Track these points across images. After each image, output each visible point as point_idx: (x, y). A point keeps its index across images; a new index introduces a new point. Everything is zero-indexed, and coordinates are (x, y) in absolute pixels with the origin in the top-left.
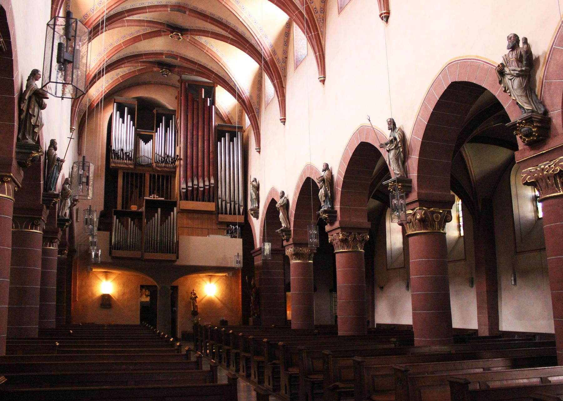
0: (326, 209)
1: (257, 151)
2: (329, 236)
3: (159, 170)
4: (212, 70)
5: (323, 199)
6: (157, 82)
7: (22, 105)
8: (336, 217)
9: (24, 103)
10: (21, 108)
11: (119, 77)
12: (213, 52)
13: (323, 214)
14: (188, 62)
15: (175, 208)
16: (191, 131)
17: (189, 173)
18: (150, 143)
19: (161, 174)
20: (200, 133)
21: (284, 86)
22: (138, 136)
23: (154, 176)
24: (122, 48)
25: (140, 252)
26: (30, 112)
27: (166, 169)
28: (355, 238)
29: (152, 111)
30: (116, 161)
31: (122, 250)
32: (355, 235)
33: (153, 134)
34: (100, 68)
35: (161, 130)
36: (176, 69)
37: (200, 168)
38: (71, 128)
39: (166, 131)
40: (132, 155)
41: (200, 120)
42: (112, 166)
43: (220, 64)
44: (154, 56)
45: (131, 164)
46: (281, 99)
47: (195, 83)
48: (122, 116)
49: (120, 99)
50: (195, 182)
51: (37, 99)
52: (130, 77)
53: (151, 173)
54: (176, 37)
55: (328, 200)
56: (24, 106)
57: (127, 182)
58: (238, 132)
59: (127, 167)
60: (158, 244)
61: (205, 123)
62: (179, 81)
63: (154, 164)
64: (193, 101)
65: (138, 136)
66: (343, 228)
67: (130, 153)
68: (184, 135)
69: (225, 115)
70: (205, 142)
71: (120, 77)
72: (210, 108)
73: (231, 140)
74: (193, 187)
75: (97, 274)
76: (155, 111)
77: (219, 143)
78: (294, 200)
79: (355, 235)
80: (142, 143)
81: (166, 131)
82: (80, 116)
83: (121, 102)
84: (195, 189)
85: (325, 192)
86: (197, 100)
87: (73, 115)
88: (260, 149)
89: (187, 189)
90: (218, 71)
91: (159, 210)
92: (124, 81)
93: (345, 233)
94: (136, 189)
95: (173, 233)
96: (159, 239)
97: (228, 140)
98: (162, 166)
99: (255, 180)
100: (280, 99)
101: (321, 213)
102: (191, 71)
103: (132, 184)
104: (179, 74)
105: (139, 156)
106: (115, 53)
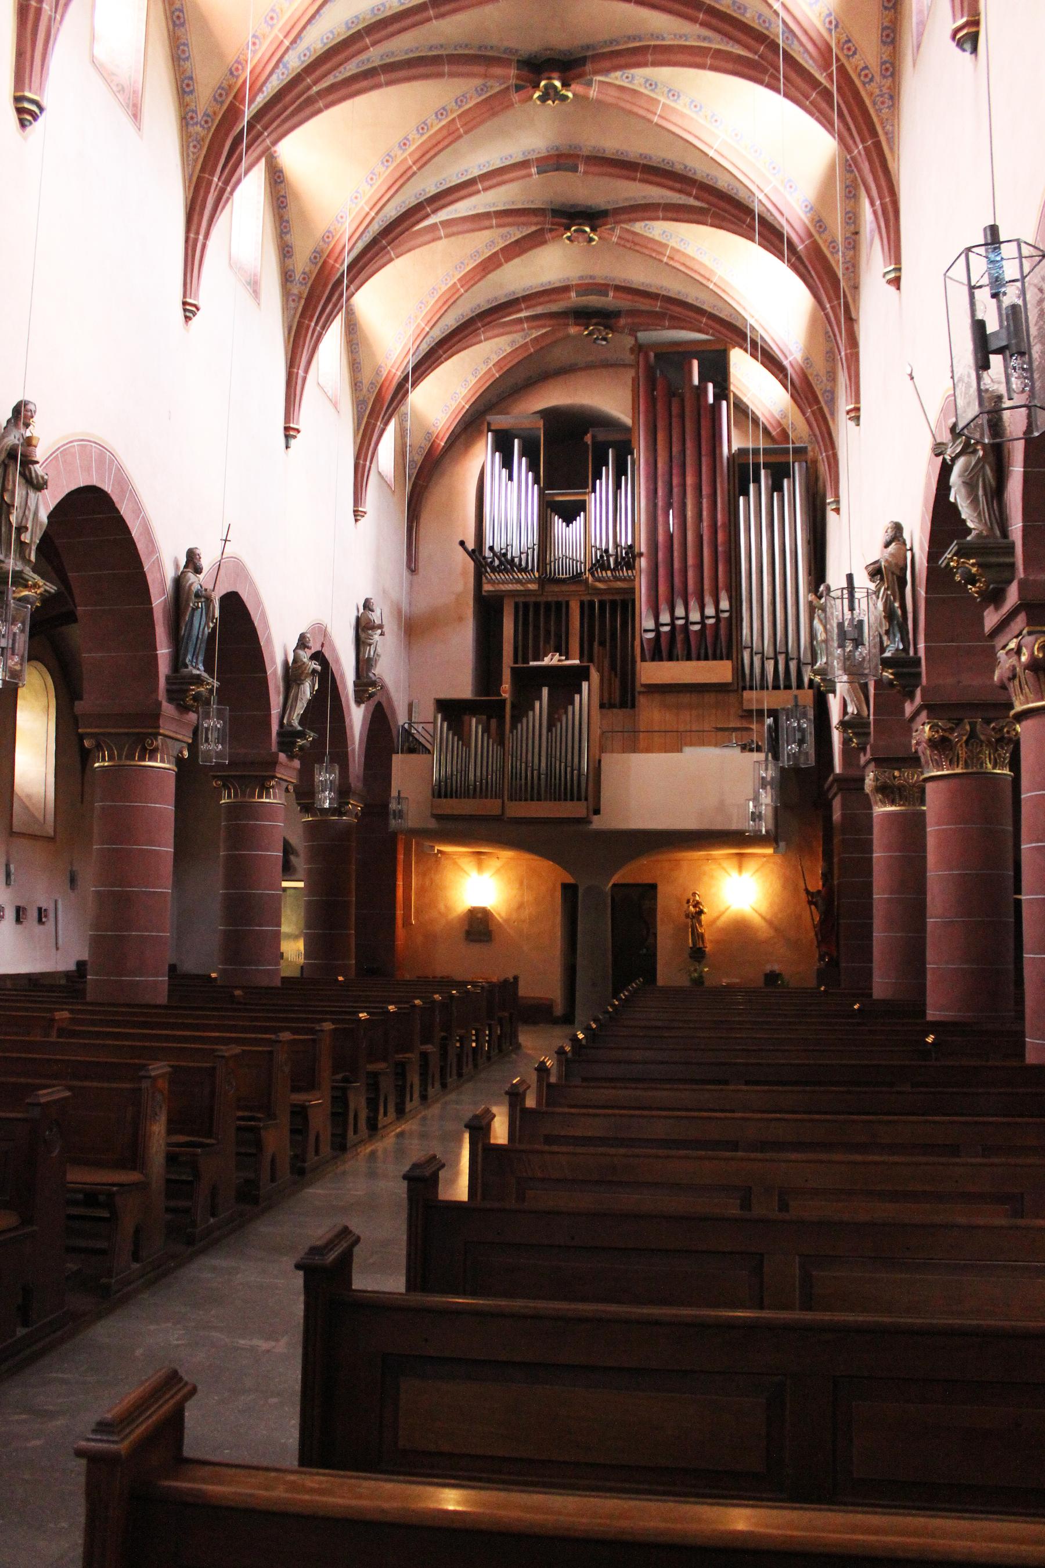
3: (600, 589)
4: (698, 305)
6: (592, 361)
8: (919, 675)
11: (491, 365)
12: (689, 257)
15: (584, 683)
16: (667, 477)
17: (662, 589)
18: (580, 521)
19: (611, 597)
20: (690, 480)
21: (854, 316)
22: (547, 507)
23: (591, 603)
25: (500, 801)
29: (582, 438)
31: (456, 797)
32: (973, 725)
33: (587, 498)
36: (622, 321)
37: (691, 574)
38: (355, 511)
39: (618, 486)
42: (486, 591)
43: (711, 286)
44: (547, 299)
45: (530, 581)
46: (846, 355)
48: (507, 463)
49: (500, 421)
50: (680, 611)
52: (516, 360)
54: (581, 239)
55: (896, 629)
58: (793, 463)
59: (522, 588)
61: (703, 452)
62: (632, 350)
65: (547, 507)
67: (530, 551)
68: (647, 489)
69: (771, 420)
70: (705, 501)
71: (494, 365)
72: (715, 409)
73: (776, 487)
74: (672, 624)
75: (459, 858)
76: (588, 439)
77: (741, 498)
79: (973, 725)
80: (558, 524)
81: (618, 486)
84: (678, 629)
87: (359, 479)
89: (657, 630)
90: (715, 306)
91: (545, 691)
92: (505, 373)
95: (580, 747)
96: (543, 765)
97: (766, 488)
102: (657, 319)
104: (633, 332)
105: (552, 559)
106: (442, 311)
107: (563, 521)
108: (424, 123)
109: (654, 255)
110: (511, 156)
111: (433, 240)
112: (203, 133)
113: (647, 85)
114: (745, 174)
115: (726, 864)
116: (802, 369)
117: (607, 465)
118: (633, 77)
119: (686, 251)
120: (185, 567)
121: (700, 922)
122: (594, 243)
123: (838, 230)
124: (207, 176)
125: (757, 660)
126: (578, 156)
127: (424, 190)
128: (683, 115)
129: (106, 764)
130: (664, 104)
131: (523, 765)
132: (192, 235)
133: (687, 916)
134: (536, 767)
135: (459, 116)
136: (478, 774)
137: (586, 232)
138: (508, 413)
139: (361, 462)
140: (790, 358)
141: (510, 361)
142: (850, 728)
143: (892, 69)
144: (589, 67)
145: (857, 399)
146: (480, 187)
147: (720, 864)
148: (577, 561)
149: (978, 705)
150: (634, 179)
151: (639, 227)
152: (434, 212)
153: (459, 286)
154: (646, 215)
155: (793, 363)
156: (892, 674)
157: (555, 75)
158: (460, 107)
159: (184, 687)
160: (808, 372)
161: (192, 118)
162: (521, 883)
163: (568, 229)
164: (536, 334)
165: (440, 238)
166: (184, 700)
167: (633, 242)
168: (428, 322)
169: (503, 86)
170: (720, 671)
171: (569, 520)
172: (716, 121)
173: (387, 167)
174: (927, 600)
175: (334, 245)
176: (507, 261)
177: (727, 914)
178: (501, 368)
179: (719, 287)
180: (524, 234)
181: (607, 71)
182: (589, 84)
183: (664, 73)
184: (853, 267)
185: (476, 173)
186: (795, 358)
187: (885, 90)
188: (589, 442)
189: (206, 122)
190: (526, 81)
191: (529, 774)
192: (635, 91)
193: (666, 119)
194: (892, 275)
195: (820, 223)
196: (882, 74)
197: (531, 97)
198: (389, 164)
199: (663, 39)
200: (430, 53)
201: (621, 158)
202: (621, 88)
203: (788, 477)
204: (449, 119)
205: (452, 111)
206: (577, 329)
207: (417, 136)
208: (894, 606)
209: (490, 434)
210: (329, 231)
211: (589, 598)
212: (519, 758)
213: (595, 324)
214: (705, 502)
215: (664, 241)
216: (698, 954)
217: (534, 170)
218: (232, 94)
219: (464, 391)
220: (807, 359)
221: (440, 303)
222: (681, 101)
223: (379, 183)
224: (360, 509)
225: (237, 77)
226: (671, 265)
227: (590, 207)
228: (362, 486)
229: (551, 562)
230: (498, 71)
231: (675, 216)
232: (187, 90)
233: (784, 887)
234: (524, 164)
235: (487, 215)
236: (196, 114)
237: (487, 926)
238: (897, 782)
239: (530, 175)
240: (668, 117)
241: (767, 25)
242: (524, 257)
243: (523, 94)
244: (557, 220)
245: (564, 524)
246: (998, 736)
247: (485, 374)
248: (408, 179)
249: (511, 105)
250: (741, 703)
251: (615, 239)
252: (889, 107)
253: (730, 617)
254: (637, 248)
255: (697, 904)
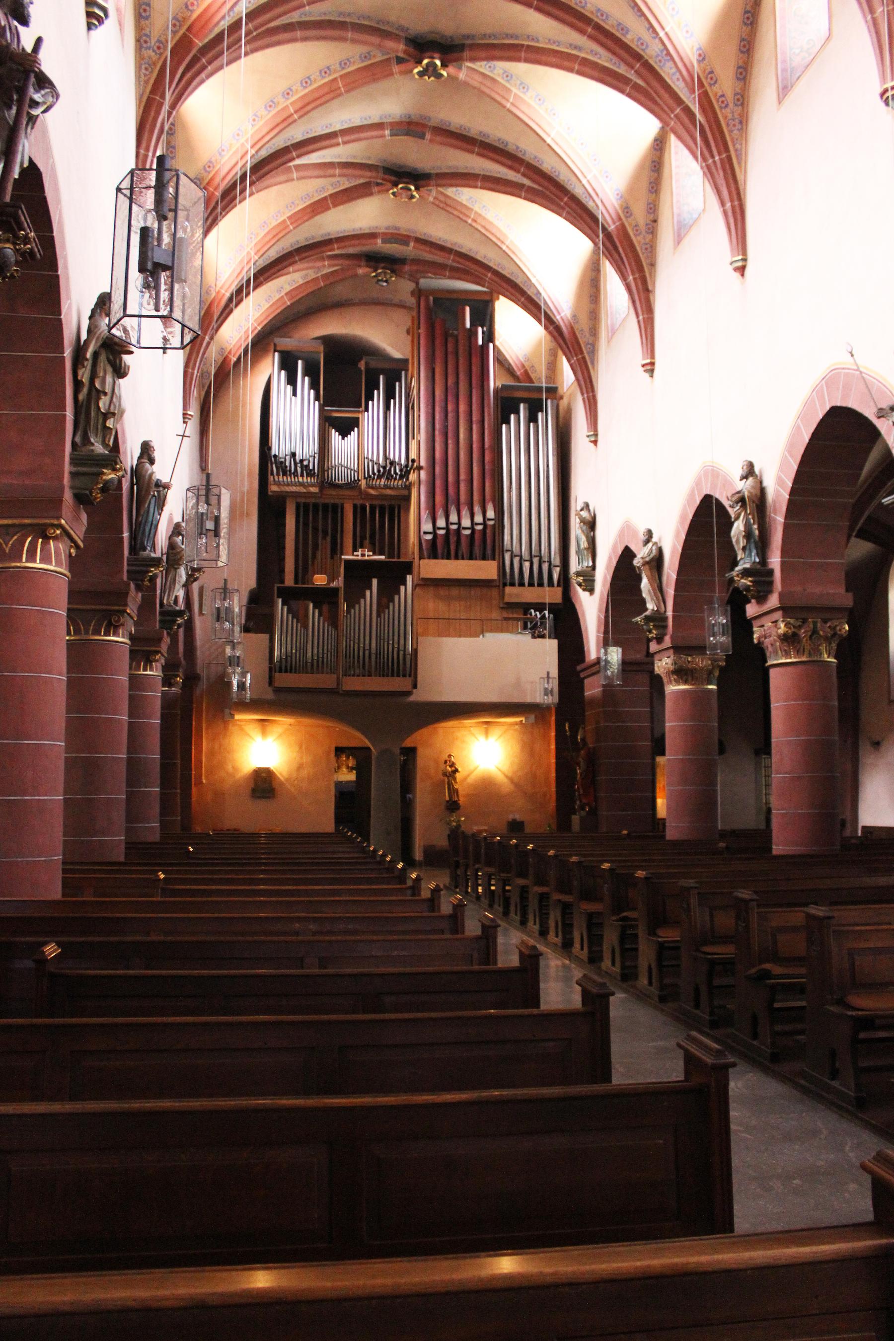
0: (748, 566)
1: (591, 442)
2: (755, 629)
3: (372, 495)
5: (742, 542)
7: (80, 372)
8: (771, 583)
9: (84, 366)
10: (79, 378)
11: (283, 294)
13: (742, 578)
14: (432, 250)
16: (443, 404)
17: (439, 498)
18: (354, 434)
20: (462, 408)
21: (650, 288)
23: (363, 508)
24: (287, 230)
26: (98, 385)
27: (389, 492)
28: (815, 632)
30: (281, 479)
32: (815, 623)
33: (360, 416)
34: (243, 278)
35: (377, 405)
36: (407, 268)
37: (463, 487)
38: (184, 414)
39: (387, 407)
40: (314, 464)
41: (462, 376)
42: (272, 491)
43: (504, 248)
45: (312, 485)
46: (644, 318)
47: (448, 296)
48: (292, 381)
49: (287, 343)
50: (453, 518)
51: (111, 357)
53: (355, 502)
55: (753, 546)
56: (84, 375)
57: (306, 524)
59: (304, 490)
60: (373, 657)
61: (474, 385)
62: (413, 293)
63: (363, 483)
64: (446, 336)
66: (786, 609)
67: (311, 459)
68: (427, 413)
72: (484, 349)
73: (532, 418)
74: (447, 528)
76: (362, 365)
77: (504, 426)
78: (674, 547)
79: (815, 623)
80: (335, 436)
81: (387, 407)
82: (203, 387)
83: (289, 348)
84: (452, 532)
85: (745, 528)
86: (455, 332)
87: (188, 386)
88: (596, 435)
89: (434, 533)
91: (375, 582)
93: (792, 621)
94: (324, 538)
97: (524, 418)
98: (379, 485)
99: (587, 506)
100: (641, 317)
101: (738, 575)
102: (439, 269)
103: (315, 529)
107: (340, 434)
108: (309, 78)
109: (461, 216)
110: (370, 118)
111: (287, 181)
112: (155, 57)
113: (505, 76)
114: (573, 162)
115: (474, 730)
116: (570, 324)
117: (378, 389)
118: (494, 68)
119: (486, 216)
120: (139, 458)
121: (455, 779)
122: (414, 200)
123: (640, 216)
124: (158, 98)
125: (516, 561)
126: (424, 126)
127: (293, 137)
128: (529, 106)
129: (72, 638)
130: (515, 94)
131: (356, 645)
132: (142, 151)
133: (445, 774)
134: (367, 647)
135: (341, 76)
136: (315, 652)
137: (410, 190)
138: (290, 337)
139: (190, 370)
140: (562, 315)
141: (300, 293)
142: (652, 621)
143: (743, 100)
144: (466, 54)
145: (653, 356)
146: (340, 140)
147: (470, 731)
148: (351, 470)
149: (829, 608)
150: (472, 152)
151: (451, 191)
152: (299, 156)
153: (289, 223)
154: (454, 182)
155: (564, 318)
156: (751, 581)
157: (436, 55)
158: (343, 68)
159: (144, 569)
160: (576, 327)
161: (146, 42)
162: (301, 747)
163: (396, 185)
164: (326, 271)
165: (293, 180)
166: (143, 581)
167: (445, 203)
168: (258, 251)
169: (385, 57)
170: (487, 570)
171: (344, 433)
172: (554, 114)
173: (270, 111)
174: (786, 527)
175: (214, 175)
176: (335, 206)
177: (475, 773)
178: (293, 297)
179: (510, 249)
180: (352, 185)
181: (473, 59)
182: (460, 68)
183: (520, 68)
184: (652, 248)
185: (338, 127)
186: (565, 315)
187: (736, 116)
188: (363, 368)
189: (159, 48)
190: (410, 56)
191: (361, 653)
192: (493, 80)
193: (515, 106)
194: (740, 264)
195: (627, 209)
196: (734, 103)
197: (411, 71)
198: (272, 109)
199: (538, 41)
200: (337, 19)
201: (464, 133)
202: (484, 75)
203: (542, 411)
204: (331, 78)
205: (335, 71)
206: (368, 270)
207: (300, 88)
208: (751, 528)
209: (276, 354)
210: (210, 162)
211: (361, 502)
212: (352, 639)
213: (383, 268)
214: (475, 428)
215: (470, 206)
216: (453, 806)
217: (387, 132)
218: (185, 27)
219: (258, 315)
220: (574, 316)
221: (270, 236)
222: (529, 94)
223: (261, 123)
224: (189, 412)
225: (192, 11)
226: (474, 227)
227: (415, 169)
228: (190, 393)
229: (328, 469)
230: (390, 44)
231: (492, 186)
232: (143, 14)
233: (523, 748)
234: (380, 126)
235: (331, 165)
236: (150, 39)
237: (271, 783)
238: (690, 666)
239: (383, 136)
240: (517, 104)
241: (644, 47)
242: (347, 206)
243: (403, 67)
244: (386, 177)
245: (340, 437)
246: (832, 633)
247: (278, 300)
248: (289, 125)
249: (391, 74)
250: (503, 598)
251: (431, 199)
252: (738, 130)
253: (494, 526)
254: (449, 209)
255: (452, 765)
